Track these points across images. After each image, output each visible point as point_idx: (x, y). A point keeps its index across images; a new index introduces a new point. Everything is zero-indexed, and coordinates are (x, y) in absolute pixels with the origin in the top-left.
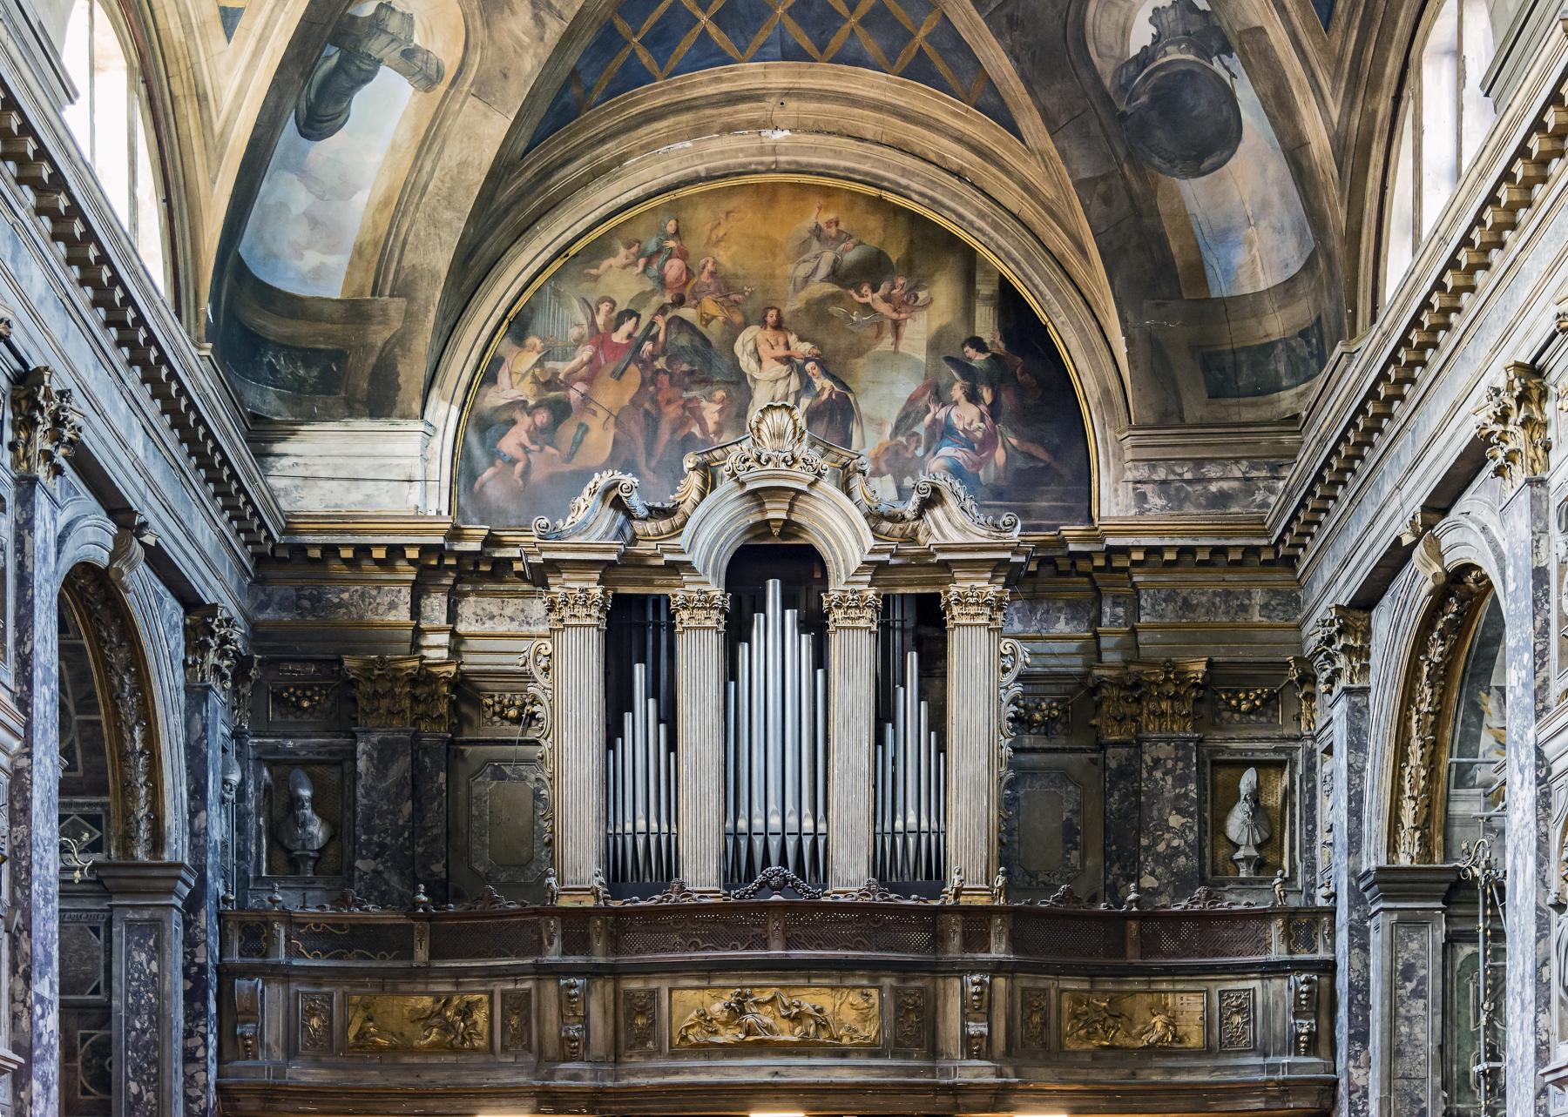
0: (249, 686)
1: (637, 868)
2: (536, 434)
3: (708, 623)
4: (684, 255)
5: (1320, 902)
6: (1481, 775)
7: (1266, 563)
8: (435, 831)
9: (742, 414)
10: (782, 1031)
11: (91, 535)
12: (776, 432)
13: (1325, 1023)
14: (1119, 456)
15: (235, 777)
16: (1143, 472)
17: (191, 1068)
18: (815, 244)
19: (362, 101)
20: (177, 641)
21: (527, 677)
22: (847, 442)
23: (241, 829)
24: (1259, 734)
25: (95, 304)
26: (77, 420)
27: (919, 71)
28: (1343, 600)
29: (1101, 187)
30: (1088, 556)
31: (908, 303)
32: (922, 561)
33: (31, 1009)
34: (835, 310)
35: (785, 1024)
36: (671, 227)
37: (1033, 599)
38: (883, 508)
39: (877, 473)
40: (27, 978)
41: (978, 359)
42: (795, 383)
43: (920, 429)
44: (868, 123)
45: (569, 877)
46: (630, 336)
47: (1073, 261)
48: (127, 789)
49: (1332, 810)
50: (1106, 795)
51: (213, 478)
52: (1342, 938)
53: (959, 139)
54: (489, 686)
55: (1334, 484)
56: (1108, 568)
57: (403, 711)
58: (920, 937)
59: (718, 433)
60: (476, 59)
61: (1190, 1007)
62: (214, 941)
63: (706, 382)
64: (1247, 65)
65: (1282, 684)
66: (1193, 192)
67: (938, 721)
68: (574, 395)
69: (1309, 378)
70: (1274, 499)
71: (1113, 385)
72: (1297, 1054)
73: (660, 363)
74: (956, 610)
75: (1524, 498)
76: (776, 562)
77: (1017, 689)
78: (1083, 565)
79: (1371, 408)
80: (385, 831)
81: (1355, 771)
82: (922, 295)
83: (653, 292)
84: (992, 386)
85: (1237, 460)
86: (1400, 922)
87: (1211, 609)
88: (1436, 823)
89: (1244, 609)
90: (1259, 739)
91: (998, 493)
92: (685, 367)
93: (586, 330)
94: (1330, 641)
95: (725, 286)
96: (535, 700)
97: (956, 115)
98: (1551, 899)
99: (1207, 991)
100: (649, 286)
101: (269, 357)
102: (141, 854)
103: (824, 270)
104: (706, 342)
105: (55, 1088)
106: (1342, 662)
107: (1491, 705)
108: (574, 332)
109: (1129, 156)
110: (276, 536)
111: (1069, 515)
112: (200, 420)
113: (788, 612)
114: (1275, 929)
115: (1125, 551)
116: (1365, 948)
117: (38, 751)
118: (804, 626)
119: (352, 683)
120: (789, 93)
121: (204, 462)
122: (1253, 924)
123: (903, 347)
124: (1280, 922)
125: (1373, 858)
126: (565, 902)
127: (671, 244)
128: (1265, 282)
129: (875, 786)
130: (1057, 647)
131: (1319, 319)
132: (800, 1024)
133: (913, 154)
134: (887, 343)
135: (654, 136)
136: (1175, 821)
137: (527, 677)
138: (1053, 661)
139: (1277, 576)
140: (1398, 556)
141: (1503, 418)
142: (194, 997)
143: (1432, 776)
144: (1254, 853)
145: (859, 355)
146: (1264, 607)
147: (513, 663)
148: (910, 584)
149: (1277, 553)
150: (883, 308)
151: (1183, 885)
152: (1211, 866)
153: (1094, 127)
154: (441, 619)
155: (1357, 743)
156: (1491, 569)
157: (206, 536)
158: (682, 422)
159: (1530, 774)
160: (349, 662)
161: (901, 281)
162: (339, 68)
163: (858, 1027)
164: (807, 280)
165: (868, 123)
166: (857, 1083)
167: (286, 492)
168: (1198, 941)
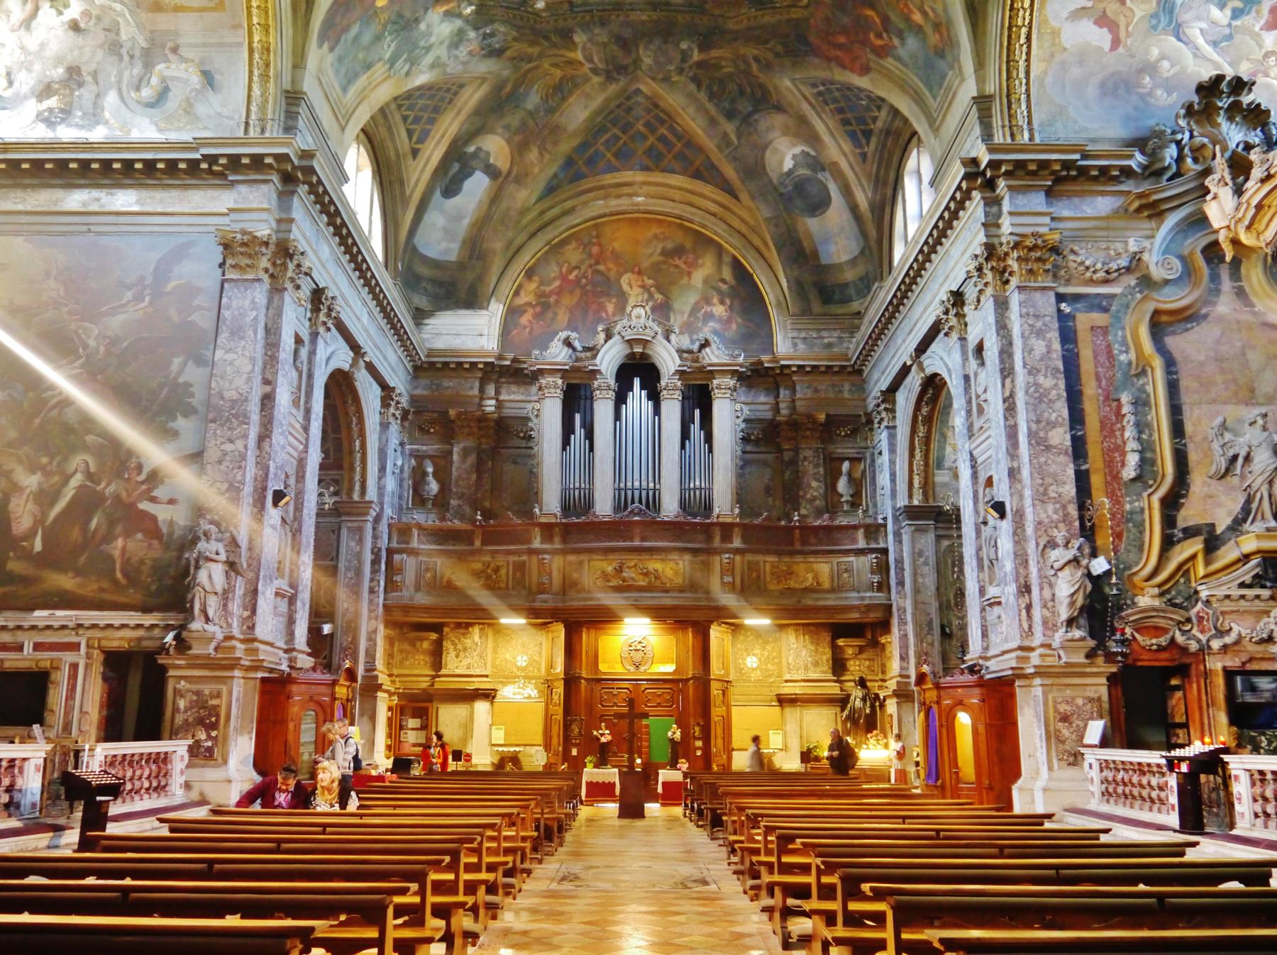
1: (578, 504)
2: (537, 316)
4: (600, 245)
5: (880, 521)
6: (947, 464)
7: (850, 373)
9: (624, 309)
11: (342, 357)
12: (638, 319)
14: (785, 327)
15: (399, 463)
16: (795, 334)
17: (373, 596)
19: (468, 184)
20: (378, 402)
21: (528, 419)
22: (668, 320)
23: (401, 486)
25: (350, 261)
26: (338, 308)
27: (697, 175)
28: (884, 388)
30: (772, 369)
31: (693, 265)
32: (701, 370)
33: (299, 568)
34: (664, 267)
35: (641, 577)
36: (594, 233)
37: (750, 387)
38: (684, 348)
39: (681, 333)
40: (298, 552)
41: (724, 287)
42: (646, 296)
43: (700, 315)
44: (677, 195)
45: (544, 508)
48: (352, 469)
49: (883, 479)
50: (783, 473)
51: (397, 333)
52: (890, 537)
53: (715, 201)
55: (877, 340)
56: (782, 374)
58: (701, 537)
59: (614, 315)
60: (515, 169)
61: (823, 569)
62: (385, 537)
63: (608, 295)
64: (832, 175)
65: (861, 425)
67: (709, 439)
68: (552, 299)
69: (865, 296)
70: (854, 346)
71: (782, 298)
73: (589, 288)
75: (958, 345)
76: (640, 369)
77: (743, 426)
78: (771, 372)
79: (891, 309)
81: (892, 462)
86: (916, 530)
87: (826, 391)
88: (927, 486)
89: (841, 392)
91: (734, 343)
94: (878, 405)
95: (616, 256)
96: (532, 429)
98: (981, 520)
102: (356, 497)
103: (659, 251)
104: (608, 279)
105: (308, 606)
106: (884, 414)
107: (950, 434)
108: (553, 275)
109: (785, 209)
111: (764, 351)
112: (392, 309)
114: (860, 534)
115: (788, 366)
116: (900, 542)
117: (311, 450)
119: (453, 421)
120: (644, 183)
121: (393, 327)
122: (850, 532)
125: (902, 501)
126: (543, 520)
134: (685, 280)
136: (814, 484)
137: (528, 419)
140: (905, 370)
141: (946, 312)
142: (376, 562)
143: (926, 465)
147: (522, 413)
148: (696, 379)
150: (683, 266)
151: (819, 513)
152: (832, 503)
154: (493, 393)
155: (892, 450)
156: (945, 375)
157: (392, 357)
158: (598, 312)
159: (968, 464)
160: (452, 413)
162: (459, 171)
164: (651, 255)
165: (677, 195)
167: (428, 340)
168: (823, 539)
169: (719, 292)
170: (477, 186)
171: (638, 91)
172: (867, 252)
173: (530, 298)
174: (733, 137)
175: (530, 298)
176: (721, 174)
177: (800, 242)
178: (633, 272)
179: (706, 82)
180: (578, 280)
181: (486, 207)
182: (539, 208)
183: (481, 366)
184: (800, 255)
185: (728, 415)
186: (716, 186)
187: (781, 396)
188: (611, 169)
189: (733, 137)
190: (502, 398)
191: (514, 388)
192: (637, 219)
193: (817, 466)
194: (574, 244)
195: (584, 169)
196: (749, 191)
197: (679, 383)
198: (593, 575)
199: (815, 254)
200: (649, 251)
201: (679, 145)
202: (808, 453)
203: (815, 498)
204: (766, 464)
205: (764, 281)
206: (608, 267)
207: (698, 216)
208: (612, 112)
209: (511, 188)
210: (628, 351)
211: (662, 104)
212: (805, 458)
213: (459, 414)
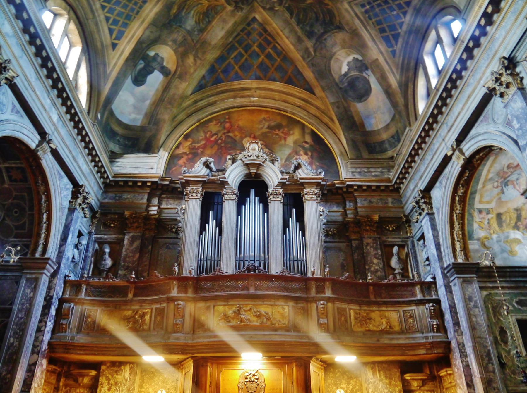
0: (96, 220)
3: (232, 198)
4: (230, 122)
7: (392, 191)
8: (146, 263)
10: (254, 321)
13: (441, 321)
14: (346, 166)
16: (354, 170)
18: (264, 122)
24: (397, 237)
29: (337, 104)
31: (288, 134)
35: (255, 319)
36: (227, 117)
41: (307, 146)
46: (215, 139)
47: (330, 124)
54: (169, 223)
57: (140, 227)
61: (394, 315)
66: (360, 107)
67: (302, 228)
70: (393, 175)
71: (343, 150)
72: (434, 332)
74: (306, 196)
76: (253, 185)
78: (340, 191)
80: (130, 262)
82: (291, 132)
83: (222, 130)
84: (311, 151)
85: (378, 167)
90: (396, 238)
92: (229, 146)
93: (204, 137)
97: (299, 92)
99: (399, 311)
100: (221, 129)
101: (118, 138)
103: (266, 126)
110: (110, 177)
113: (256, 198)
115: (351, 186)
118: (260, 201)
123: (287, 143)
124: (419, 286)
127: (227, 120)
128: (380, 126)
129: (283, 246)
130: (334, 214)
131: (397, 131)
132: (260, 318)
133: (288, 103)
134: (283, 142)
135: (224, 97)
138: (333, 218)
139: (394, 195)
144: (401, 271)
145: (276, 144)
146: (392, 203)
149: (394, 187)
150: (281, 134)
153: (334, 90)
161: (286, 129)
163: (281, 320)
164: (262, 128)
166: (281, 341)
169: (304, 148)
170: (156, 79)
171: (254, 19)
172: (397, 116)
173: (186, 150)
174: (312, 51)
175: (186, 150)
176: (304, 78)
177: (352, 117)
178: (250, 137)
179: (295, 12)
180: (216, 141)
181: (160, 93)
182: (194, 98)
183: (149, 184)
184: (354, 126)
185: (313, 211)
186: (301, 87)
187: (348, 207)
188: (238, 78)
189: (312, 51)
190: (162, 207)
191: (171, 201)
192: (254, 110)
193: (376, 249)
194: (214, 122)
195: (222, 76)
196: (322, 86)
197: (281, 191)
198: (217, 322)
199: (363, 125)
200: (261, 126)
201: (279, 60)
202: (370, 241)
203: (377, 271)
204: (340, 250)
205: (332, 142)
206: (237, 135)
207: (289, 108)
208: (238, 35)
209: (176, 82)
210: (246, 172)
211: (268, 28)
212: (368, 244)
213: (131, 215)
